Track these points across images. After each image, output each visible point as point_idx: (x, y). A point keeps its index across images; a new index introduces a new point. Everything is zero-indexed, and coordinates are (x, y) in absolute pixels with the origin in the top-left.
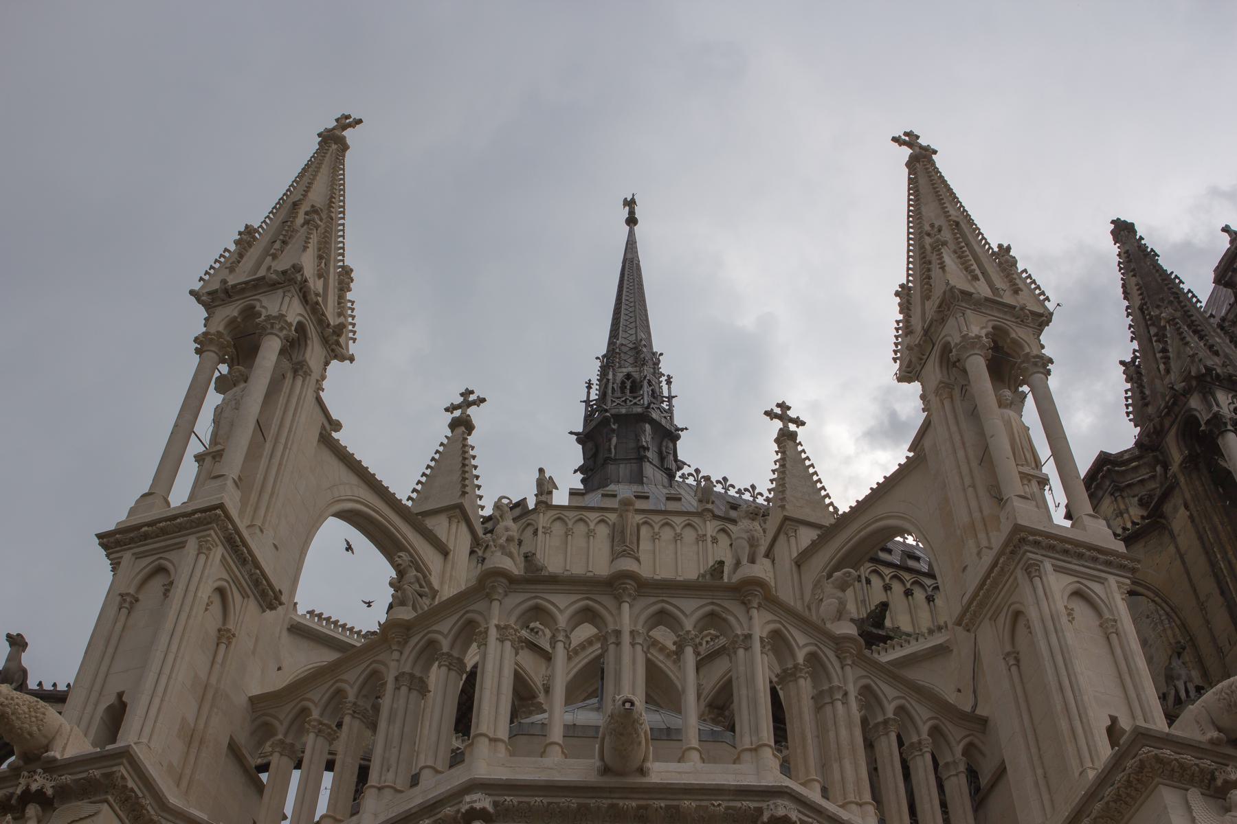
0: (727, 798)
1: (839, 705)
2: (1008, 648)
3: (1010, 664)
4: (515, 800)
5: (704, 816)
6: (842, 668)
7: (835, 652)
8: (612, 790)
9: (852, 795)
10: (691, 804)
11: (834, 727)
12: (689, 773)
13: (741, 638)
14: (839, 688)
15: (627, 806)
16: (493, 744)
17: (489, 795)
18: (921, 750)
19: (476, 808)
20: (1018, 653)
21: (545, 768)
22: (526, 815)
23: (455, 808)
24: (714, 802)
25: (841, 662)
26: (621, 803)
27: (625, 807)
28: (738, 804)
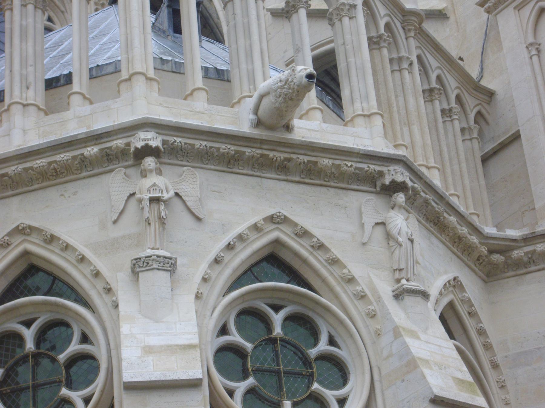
0: (355, 160)
1: (406, 73)
2: (531, 39)
3: (532, 54)
4: (184, 141)
5: (335, 173)
6: (406, 39)
7: (402, 24)
8: (262, 142)
9: (421, 159)
10: (328, 162)
11: (402, 95)
12: (317, 131)
13: (347, 7)
14: (408, 58)
15: (277, 158)
16: (149, 81)
17: (159, 134)
18: (450, 116)
19: (151, 146)
20: (539, 45)
21: (197, 112)
22: (188, 155)
23: (125, 141)
24: (347, 163)
25: (406, 34)
26: (271, 154)
27: (275, 158)
28: (364, 166)
